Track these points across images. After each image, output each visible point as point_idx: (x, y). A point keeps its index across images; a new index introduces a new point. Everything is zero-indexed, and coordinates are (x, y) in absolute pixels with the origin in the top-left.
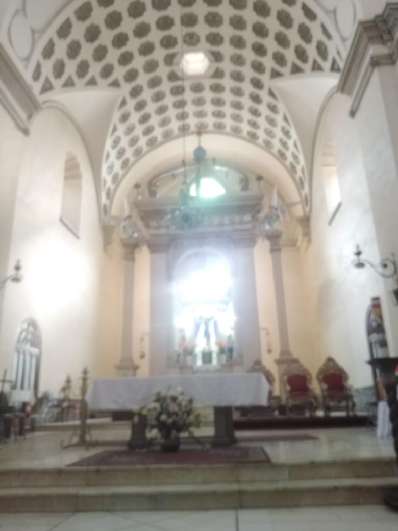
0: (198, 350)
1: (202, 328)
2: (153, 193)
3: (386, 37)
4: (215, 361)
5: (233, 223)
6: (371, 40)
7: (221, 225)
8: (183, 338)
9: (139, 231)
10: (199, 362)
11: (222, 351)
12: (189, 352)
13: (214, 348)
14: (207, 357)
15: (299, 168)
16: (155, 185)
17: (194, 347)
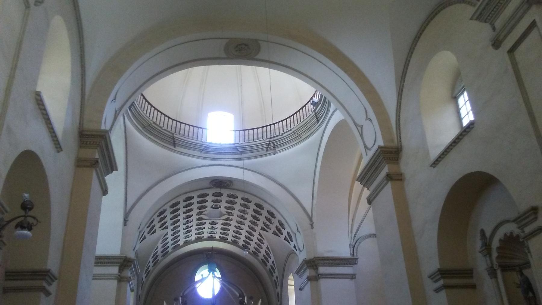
3: (315, 267)
6: (308, 267)
15: (275, 275)
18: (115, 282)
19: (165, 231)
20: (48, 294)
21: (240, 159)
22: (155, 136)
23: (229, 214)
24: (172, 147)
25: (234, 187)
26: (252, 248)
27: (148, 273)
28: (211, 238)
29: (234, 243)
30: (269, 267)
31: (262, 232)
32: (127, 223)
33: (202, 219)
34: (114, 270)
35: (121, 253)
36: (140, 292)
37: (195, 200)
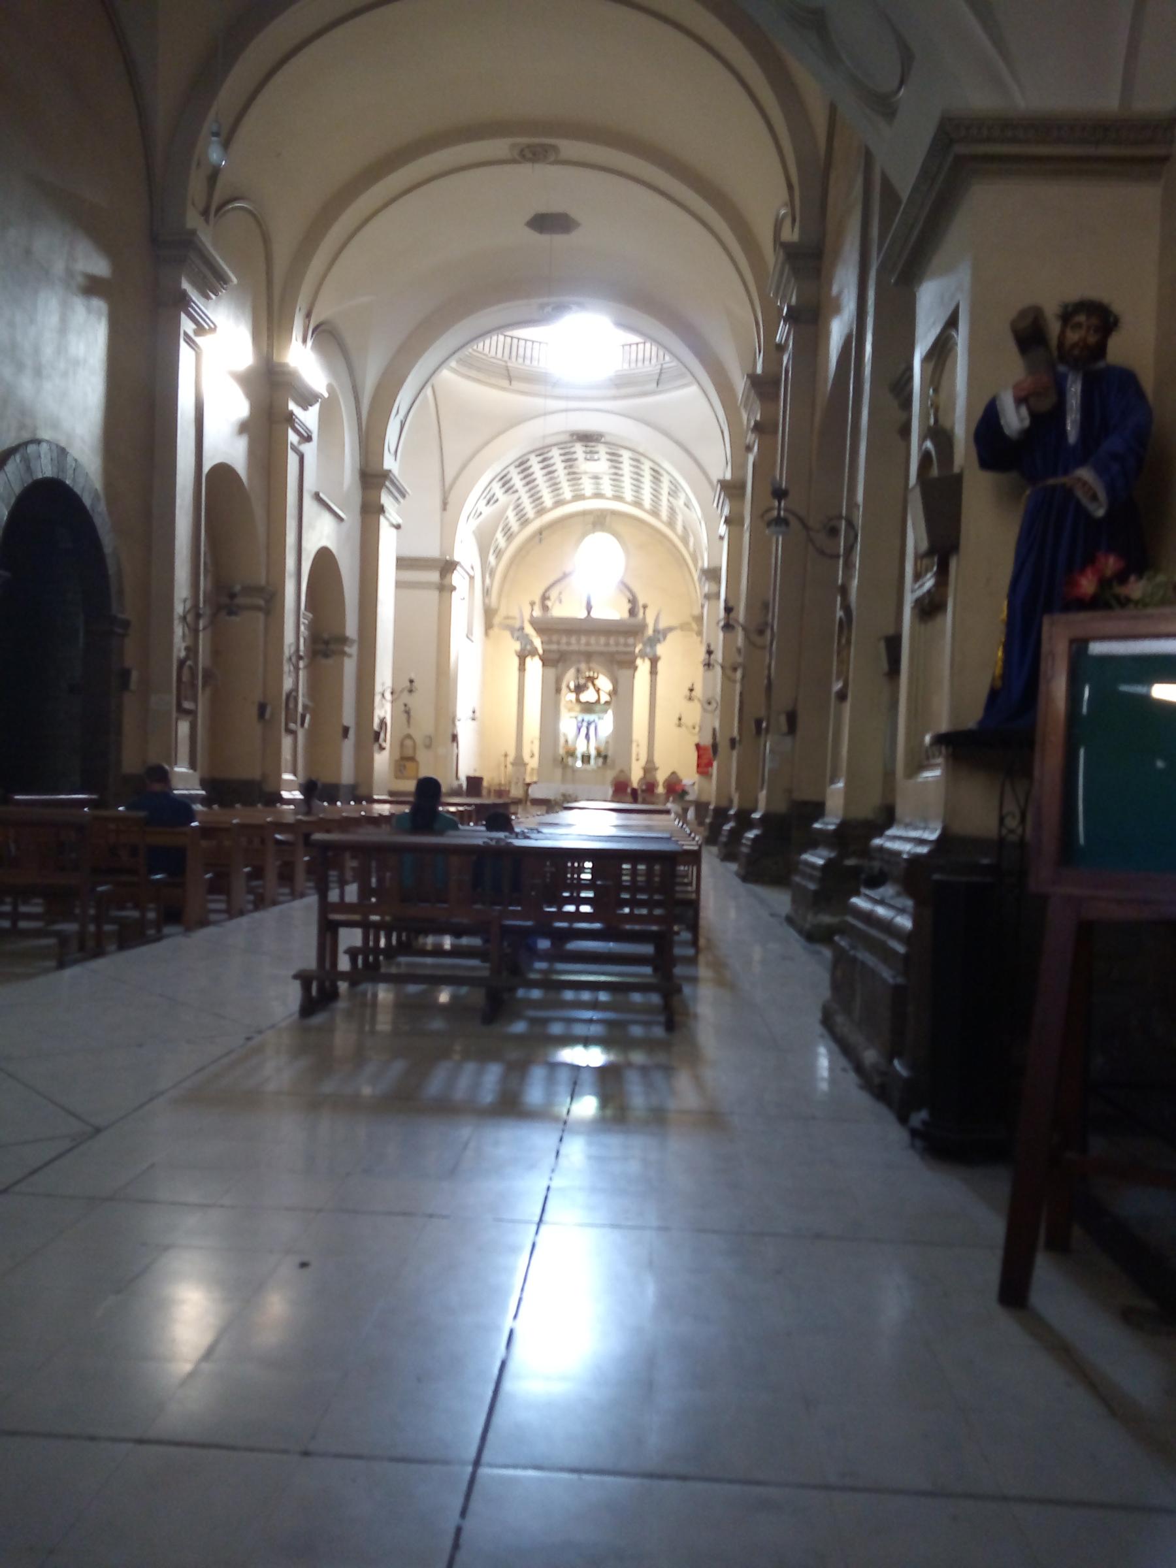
0: (579, 753)
1: (584, 731)
2: (545, 608)
4: (592, 761)
5: (617, 644)
7: (607, 644)
8: (567, 741)
9: (531, 643)
10: (579, 764)
11: (599, 754)
12: (571, 754)
13: (593, 753)
14: (586, 758)
16: (548, 598)
17: (575, 749)
18: (436, 593)
19: (516, 496)
20: (350, 656)
21: (615, 398)
22: (479, 369)
23: (616, 468)
24: (505, 383)
25: (608, 438)
26: (664, 514)
27: (499, 554)
28: (598, 495)
29: (638, 504)
30: (691, 549)
31: (671, 499)
32: (448, 507)
33: (574, 473)
34: (434, 576)
35: (442, 553)
36: (488, 581)
37: (555, 453)
